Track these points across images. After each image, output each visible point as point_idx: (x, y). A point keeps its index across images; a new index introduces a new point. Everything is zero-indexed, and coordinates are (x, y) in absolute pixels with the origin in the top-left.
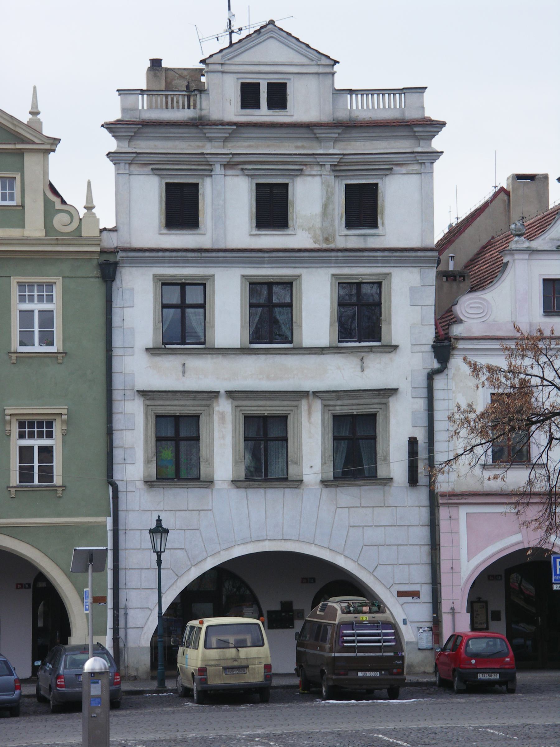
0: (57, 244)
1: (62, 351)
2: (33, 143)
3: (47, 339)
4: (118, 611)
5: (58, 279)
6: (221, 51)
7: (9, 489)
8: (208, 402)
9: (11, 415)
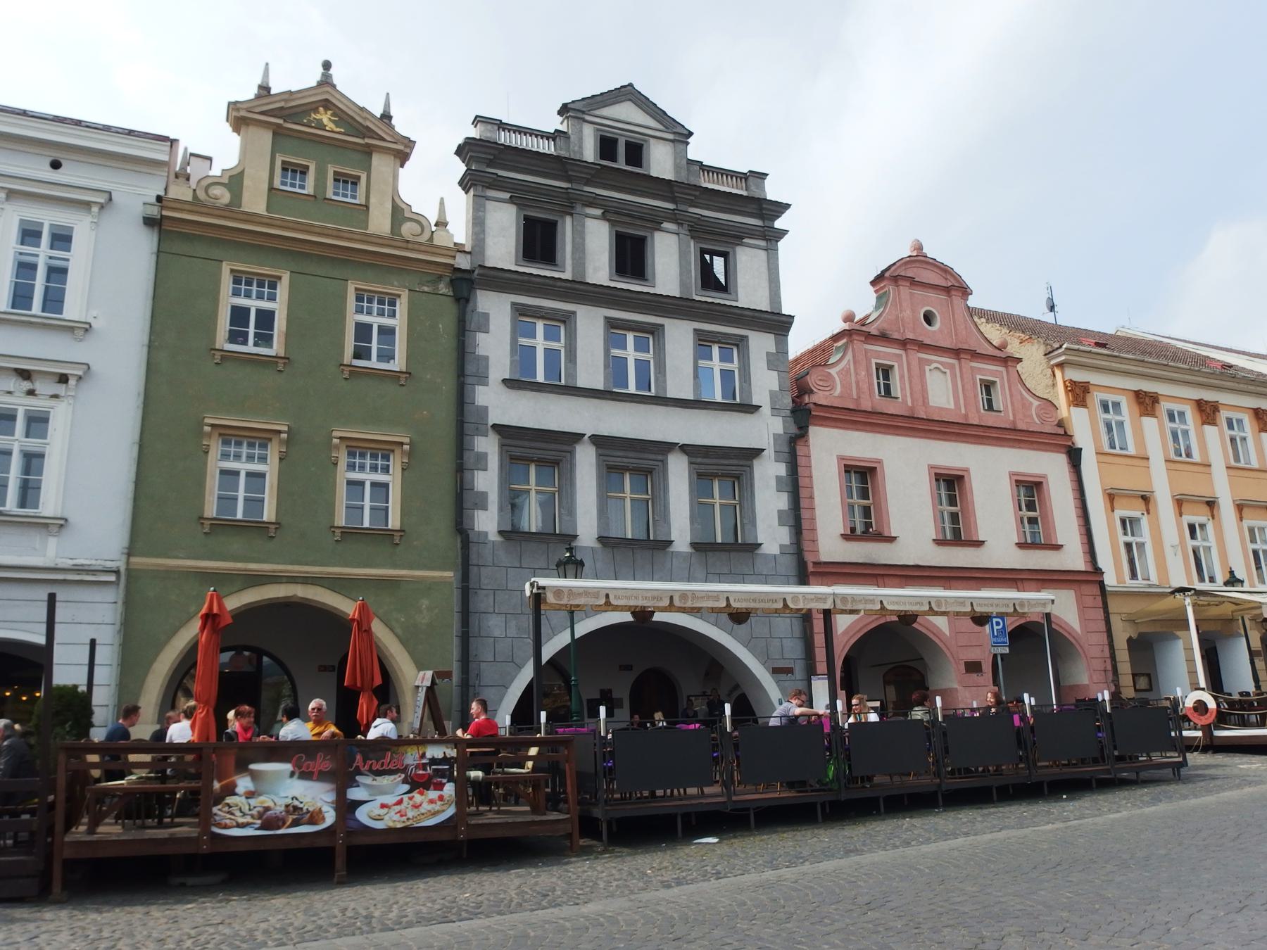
0: (407, 249)
1: (405, 370)
2: (384, 140)
3: (387, 356)
4: (468, 690)
5: (404, 291)
6: (583, 99)
7: (333, 529)
8: (565, 448)
9: (340, 438)
